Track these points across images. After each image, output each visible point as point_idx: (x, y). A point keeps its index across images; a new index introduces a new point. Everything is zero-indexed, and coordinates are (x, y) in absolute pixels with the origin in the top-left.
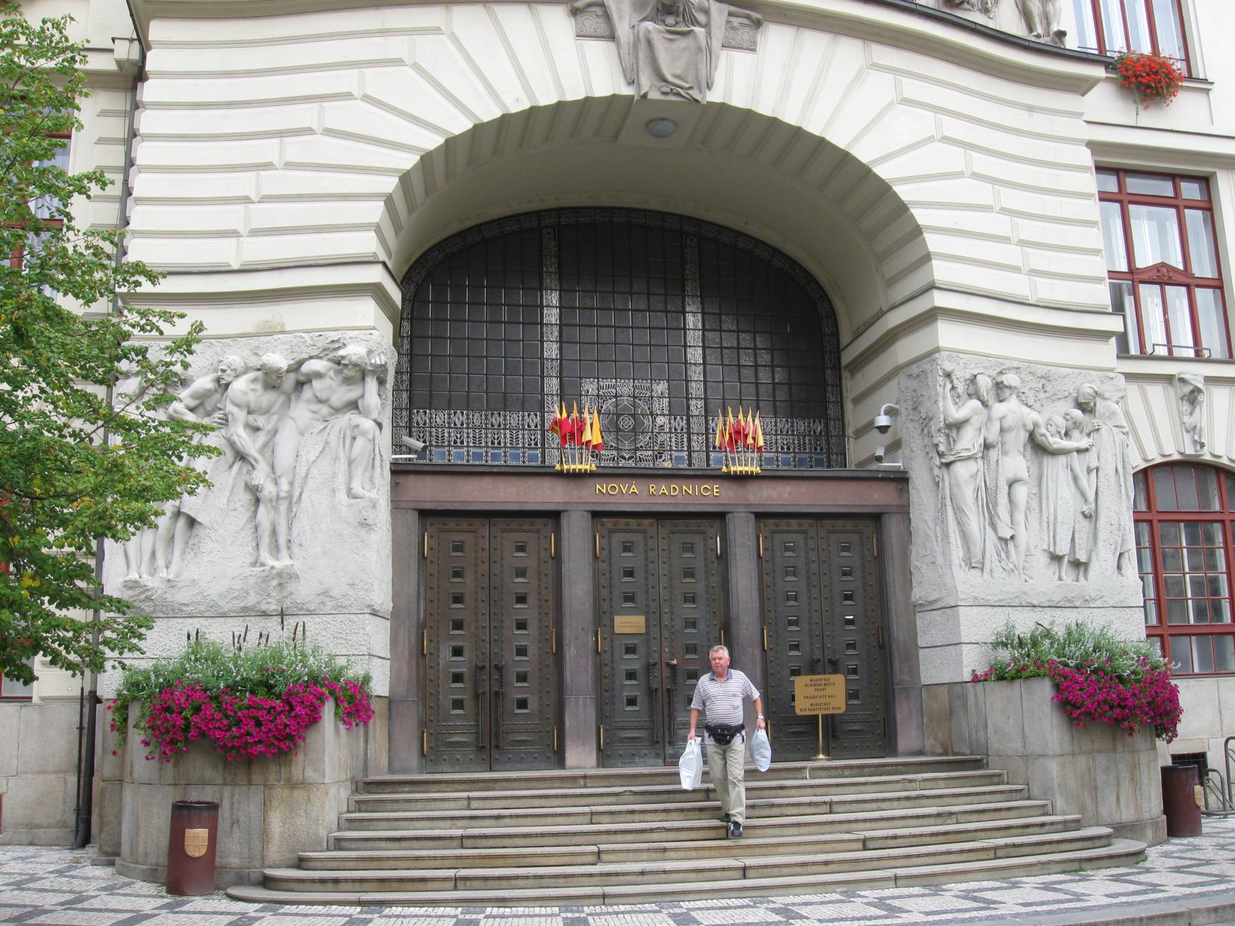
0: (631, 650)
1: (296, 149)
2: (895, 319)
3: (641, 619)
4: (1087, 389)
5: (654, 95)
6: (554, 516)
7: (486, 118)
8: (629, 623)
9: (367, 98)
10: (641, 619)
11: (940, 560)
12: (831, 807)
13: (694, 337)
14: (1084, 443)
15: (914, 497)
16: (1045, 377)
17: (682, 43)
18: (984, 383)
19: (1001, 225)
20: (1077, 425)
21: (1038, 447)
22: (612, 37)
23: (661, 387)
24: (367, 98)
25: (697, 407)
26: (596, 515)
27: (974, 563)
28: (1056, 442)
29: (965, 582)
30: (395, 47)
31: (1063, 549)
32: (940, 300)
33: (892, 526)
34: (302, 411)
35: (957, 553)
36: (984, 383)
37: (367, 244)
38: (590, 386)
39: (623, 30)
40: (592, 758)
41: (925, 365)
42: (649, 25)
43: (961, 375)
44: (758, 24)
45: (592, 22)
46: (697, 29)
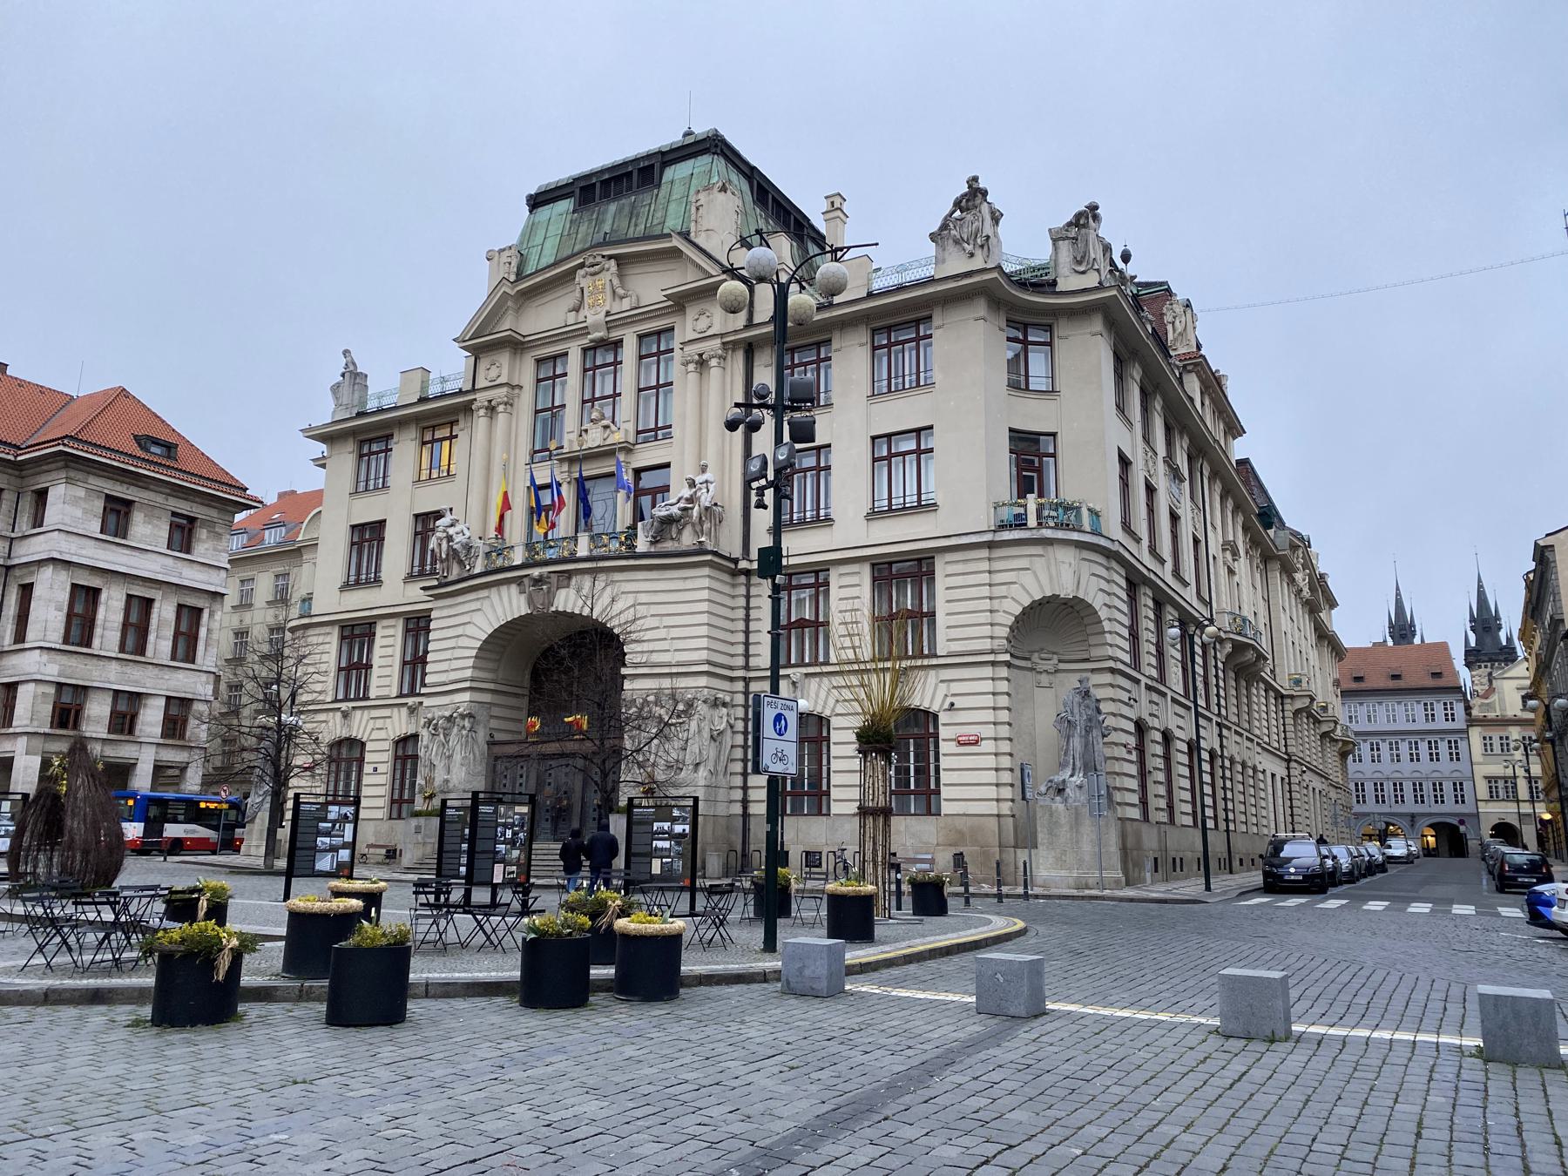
5: (535, 613)
17: (541, 592)
19: (662, 633)
32: (624, 671)
34: (455, 730)
37: (468, 673)
44: (569, 578)
45: (522, 587)
46: (544, 587)
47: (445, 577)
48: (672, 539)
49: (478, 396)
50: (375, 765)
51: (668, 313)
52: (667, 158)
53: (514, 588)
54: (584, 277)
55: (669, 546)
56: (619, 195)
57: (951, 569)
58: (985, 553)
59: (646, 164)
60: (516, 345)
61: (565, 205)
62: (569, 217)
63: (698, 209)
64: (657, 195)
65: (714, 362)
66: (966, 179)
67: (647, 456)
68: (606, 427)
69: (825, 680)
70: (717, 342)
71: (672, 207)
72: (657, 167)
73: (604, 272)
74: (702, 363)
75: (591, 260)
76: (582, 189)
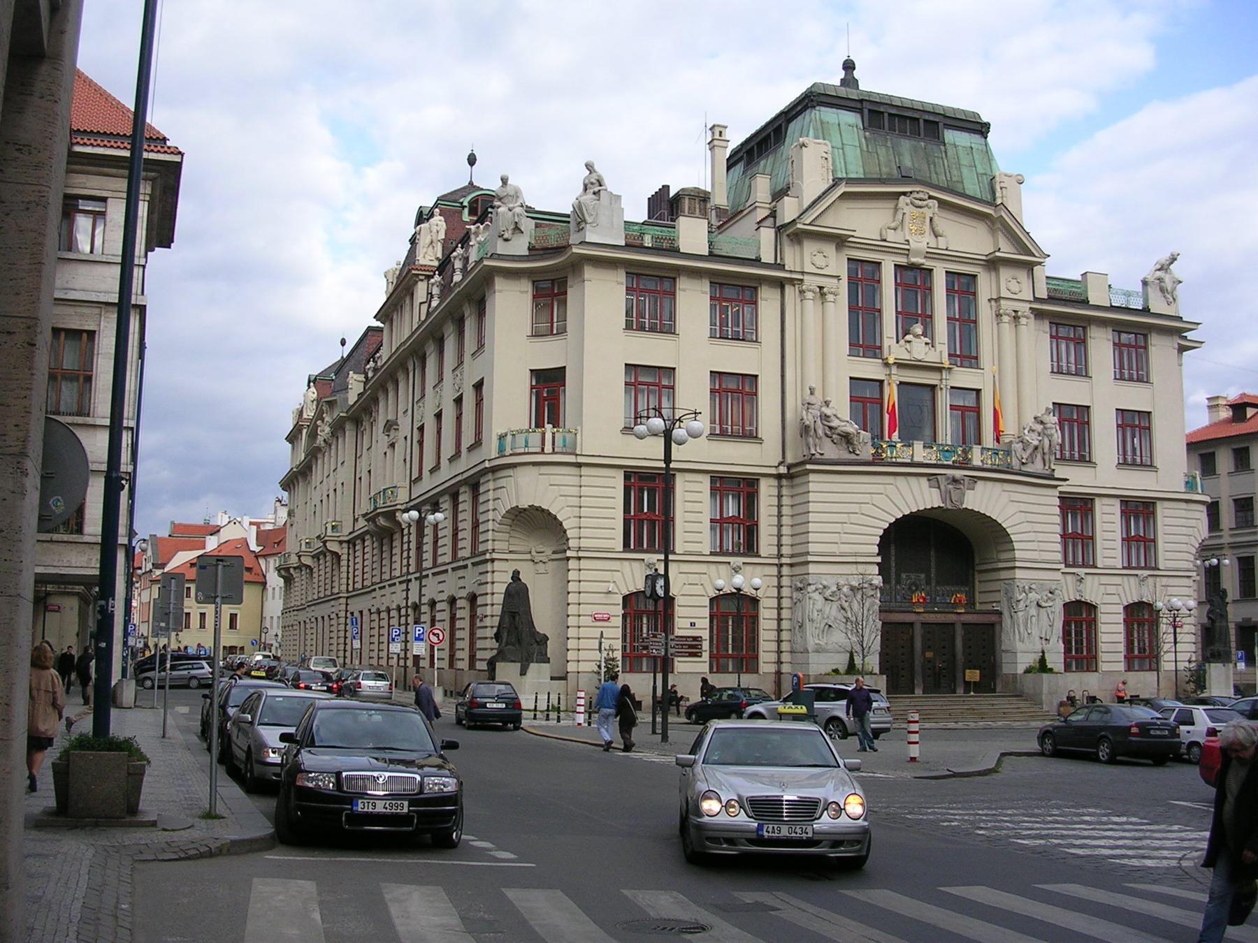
0: (929, 662)
1: (854, 518)
2: (1001, 565)
3: (932, 654)
4: (1053, 587)
5: (950, 507)
6: (911, 624)
7: (906, 513)
8: (929, 655)
9: (873, 504)
10: (932, 654)
11: (1012, 638)
12: (993, 705)
13: (933, 559)
14: (1051, 604)
15: (1004, 619)
16: (1042, 584)
18: (1027, 587)
19: (1031, 536)
20: (1049, 598)
21: (1039, 605)
22: (939, 488)
23: (923, 576)
24: (873, 504)
25: (933, 584)
26: (922, 623)
27: (1022, 641)
28: (1043, 604)
29: (1019, 646)
30: (880, 488)
31: (1043, 636)
33: (997, 627)
35: (1017, 637)
36: (1027, 587)
38: (904, 576)
39: (942, 487)
40: (921, 692)
41: (1011, 582)
42: (950, 486)
43: (1021, 586)
45: (934, 483)
47: (822, 454)
48: (1033, 463)
49: (806, 277)
50: (693, 620)
51: (980, 265)
52: (949, 122)
53: (924, 481)
54: (907, 205)
55: (1029, 468)
56: (903, 133)
57: (1167, 512)
58: (1183, 505)
59: (931, 118)
60: (840, 241)
61: (851, 118)
62: (861, 133)
63: (1001, 188)
64: (946, 152)
65: (1023, 321)
66: (1171, 251)
67: (964, 377)
68: (926, 344)
69: (1096, 577)
70: (1029, 306)
71: (965, 171)
72: (941, 125)
73: (926, 208)
74: (1016, 318)
75: (921, 196)
76: (870, 111)
